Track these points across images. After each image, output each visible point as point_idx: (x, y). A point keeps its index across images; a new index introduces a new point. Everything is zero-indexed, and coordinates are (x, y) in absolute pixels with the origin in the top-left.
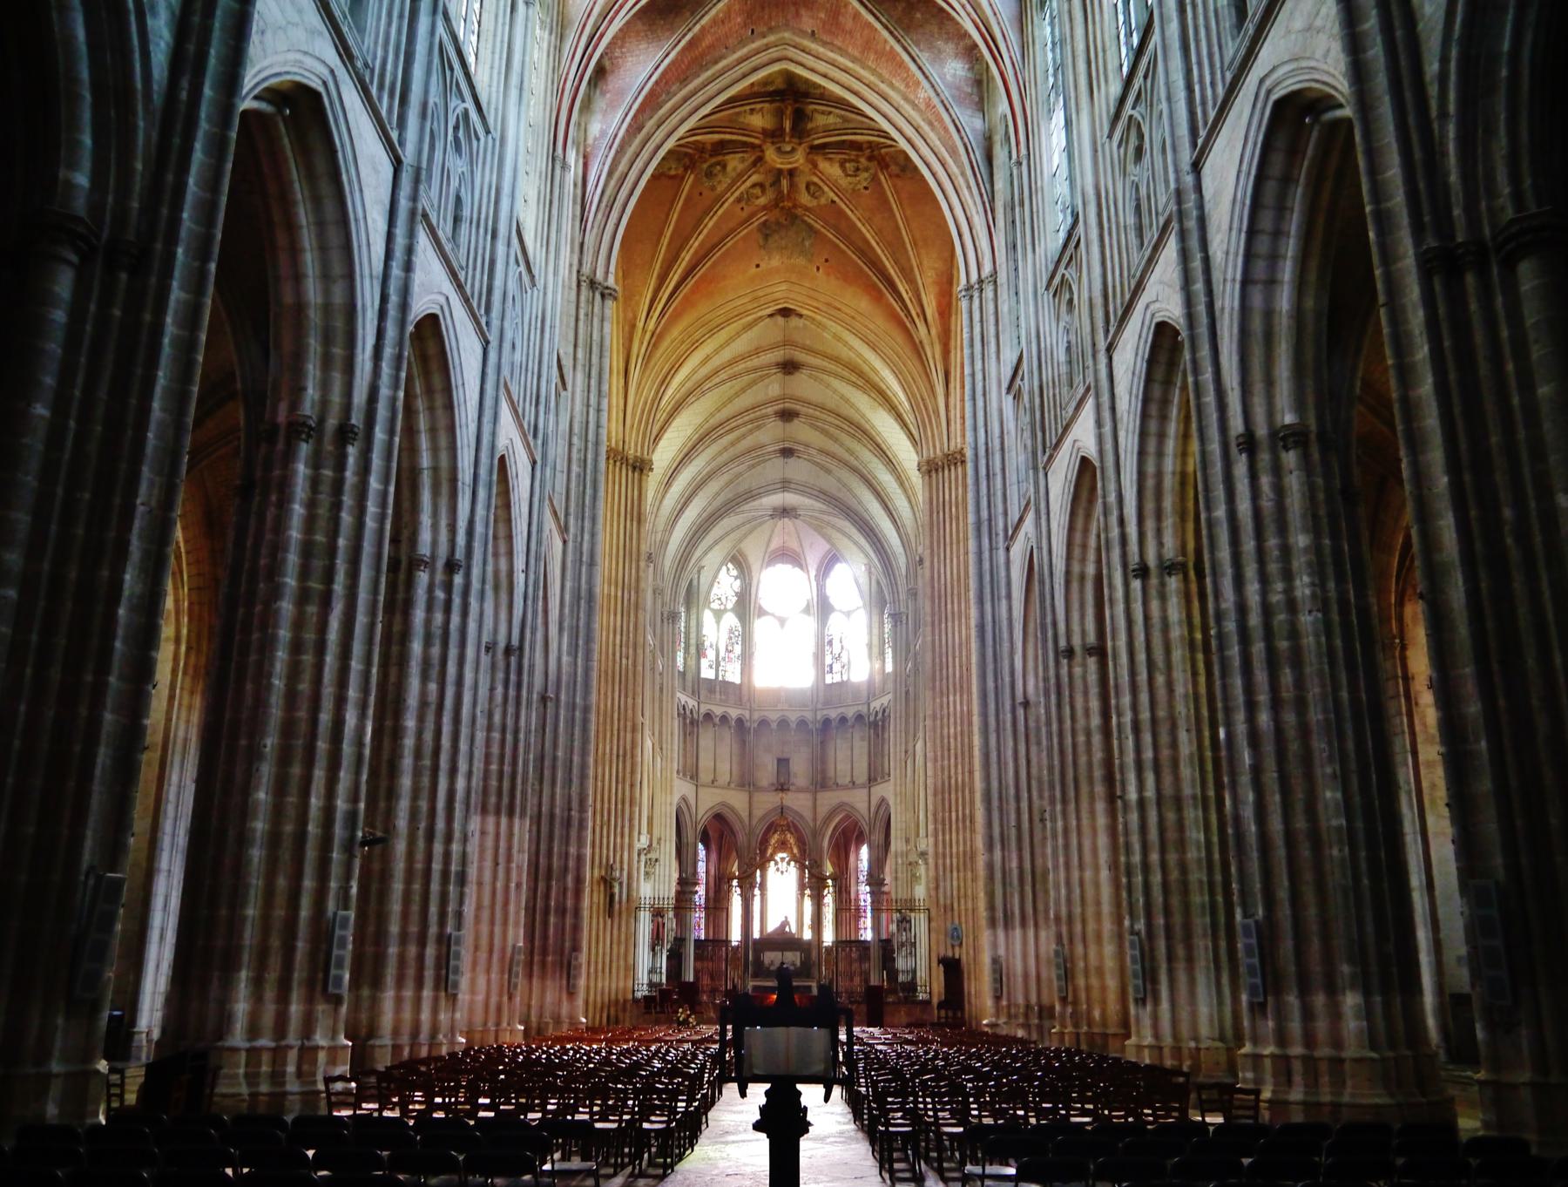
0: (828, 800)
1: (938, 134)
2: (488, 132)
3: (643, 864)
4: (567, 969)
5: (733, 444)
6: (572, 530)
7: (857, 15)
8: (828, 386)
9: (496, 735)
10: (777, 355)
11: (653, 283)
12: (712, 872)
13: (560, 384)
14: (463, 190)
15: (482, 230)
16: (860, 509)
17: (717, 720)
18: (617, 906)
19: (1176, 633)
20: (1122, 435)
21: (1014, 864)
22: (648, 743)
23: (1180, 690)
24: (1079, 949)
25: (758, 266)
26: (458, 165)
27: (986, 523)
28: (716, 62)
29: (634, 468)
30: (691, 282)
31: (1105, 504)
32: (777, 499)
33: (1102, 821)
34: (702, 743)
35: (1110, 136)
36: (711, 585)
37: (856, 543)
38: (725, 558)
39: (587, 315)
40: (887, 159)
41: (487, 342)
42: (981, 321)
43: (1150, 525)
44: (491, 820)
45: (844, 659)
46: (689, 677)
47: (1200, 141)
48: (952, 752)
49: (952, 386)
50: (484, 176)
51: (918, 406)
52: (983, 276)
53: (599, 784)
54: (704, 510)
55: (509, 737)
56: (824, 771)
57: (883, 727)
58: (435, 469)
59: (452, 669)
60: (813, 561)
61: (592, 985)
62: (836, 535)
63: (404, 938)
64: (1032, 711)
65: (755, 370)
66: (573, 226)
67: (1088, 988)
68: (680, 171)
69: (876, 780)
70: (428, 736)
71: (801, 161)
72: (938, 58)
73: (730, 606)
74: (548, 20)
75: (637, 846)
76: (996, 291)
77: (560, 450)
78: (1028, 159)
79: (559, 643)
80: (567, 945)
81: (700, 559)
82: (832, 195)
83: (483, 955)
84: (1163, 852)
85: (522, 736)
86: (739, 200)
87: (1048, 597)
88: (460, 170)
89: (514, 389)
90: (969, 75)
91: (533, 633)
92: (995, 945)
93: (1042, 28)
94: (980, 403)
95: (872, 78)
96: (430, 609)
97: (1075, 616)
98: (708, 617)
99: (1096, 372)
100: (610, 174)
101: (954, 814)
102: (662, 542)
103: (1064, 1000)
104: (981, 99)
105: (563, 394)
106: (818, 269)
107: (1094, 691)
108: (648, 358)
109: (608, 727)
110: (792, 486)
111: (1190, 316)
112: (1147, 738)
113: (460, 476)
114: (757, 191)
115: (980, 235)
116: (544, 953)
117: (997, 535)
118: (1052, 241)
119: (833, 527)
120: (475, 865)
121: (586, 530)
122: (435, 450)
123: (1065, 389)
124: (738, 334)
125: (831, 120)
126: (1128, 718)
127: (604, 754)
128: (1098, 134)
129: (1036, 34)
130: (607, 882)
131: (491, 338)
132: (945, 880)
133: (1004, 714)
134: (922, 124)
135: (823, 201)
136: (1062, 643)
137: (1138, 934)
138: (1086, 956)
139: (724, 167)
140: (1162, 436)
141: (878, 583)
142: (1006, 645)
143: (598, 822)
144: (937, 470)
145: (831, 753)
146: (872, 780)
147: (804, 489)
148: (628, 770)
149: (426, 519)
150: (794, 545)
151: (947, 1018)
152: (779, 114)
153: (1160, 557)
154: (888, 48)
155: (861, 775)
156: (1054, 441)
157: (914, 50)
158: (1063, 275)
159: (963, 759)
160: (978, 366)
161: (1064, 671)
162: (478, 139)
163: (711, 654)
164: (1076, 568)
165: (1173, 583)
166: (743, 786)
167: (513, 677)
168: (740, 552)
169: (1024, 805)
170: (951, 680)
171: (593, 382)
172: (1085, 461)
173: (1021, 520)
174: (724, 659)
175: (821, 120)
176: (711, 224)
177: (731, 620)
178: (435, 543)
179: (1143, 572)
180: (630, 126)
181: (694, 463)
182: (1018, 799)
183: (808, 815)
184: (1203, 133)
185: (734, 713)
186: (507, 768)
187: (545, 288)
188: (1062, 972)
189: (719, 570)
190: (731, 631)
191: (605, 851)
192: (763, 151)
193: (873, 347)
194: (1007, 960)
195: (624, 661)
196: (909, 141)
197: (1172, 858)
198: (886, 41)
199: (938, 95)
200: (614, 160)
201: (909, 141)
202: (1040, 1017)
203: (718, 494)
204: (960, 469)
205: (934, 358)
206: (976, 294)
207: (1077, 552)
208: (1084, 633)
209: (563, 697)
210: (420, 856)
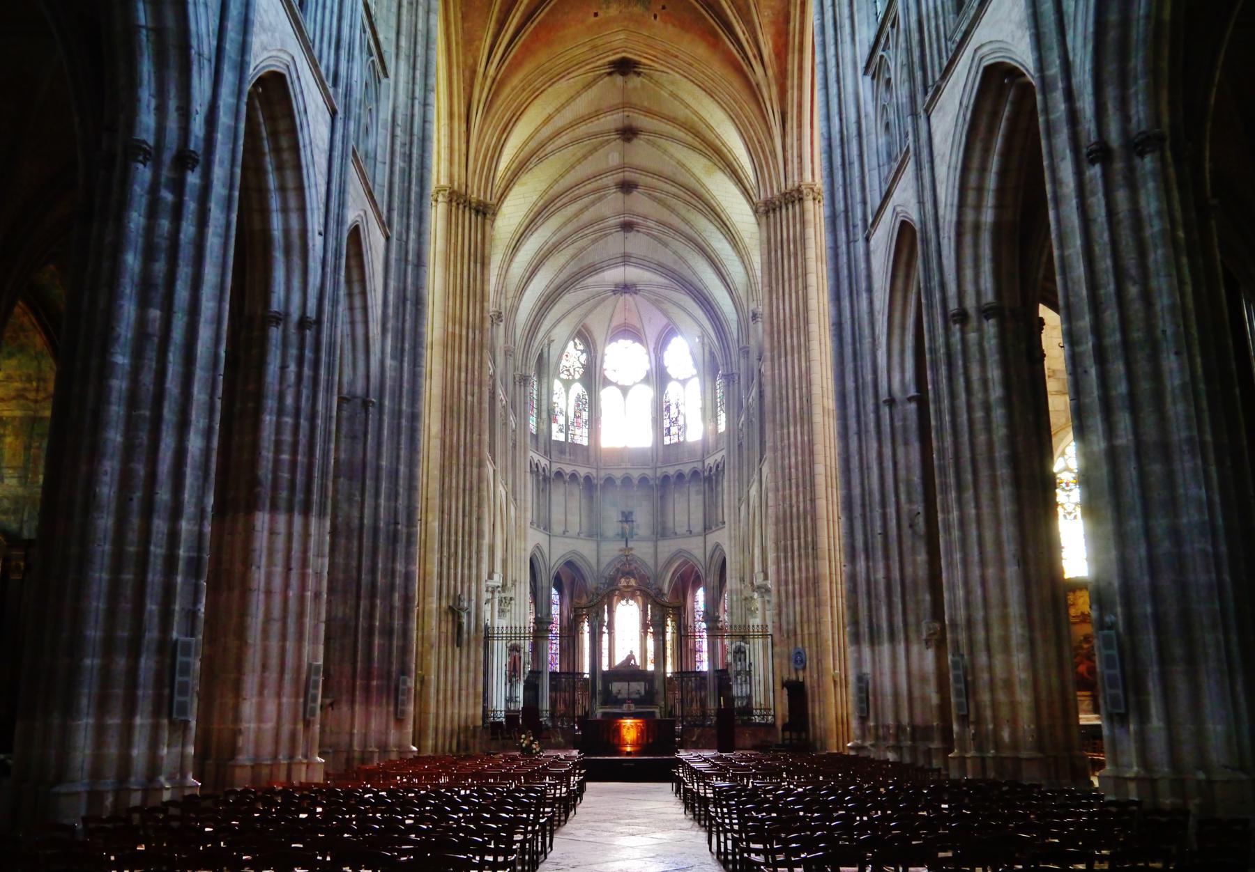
3: (496, 601)
5: (576, 215)
6: (396, 226)
8: (665, 152)
9: (288, 420)
10: (619, 176)
11: (492, 26)
12: (565, 614)
13: (379, 67)
16: (695, 281)
17: (567, 478)
18: (465, 636)
21: (880, 575)
22: (501, 489)
25: (596, 15)
27: (842, 215)
29: (477, 212)
30: (531, 27)
32: (615, 274)
34: (553, 497)
36: (560, 357)
37: (690, 315)
38: (572, 332)
44: (282, 519)
45: (681, 422)
46: (542, 440)
48: (794, 481)
49: (788, 126)
51: (755, 148)
53: (446, 517)
54: (552, 282)
56: (663, 523)
57: (717, 482)
58: (158, 31)
59: (182, 293)
60: (651, 333)
62: (674, 311)
63: (109, 646)
64: (899, 409)
65: (595, 135)
70: (147, 378)
73: (577, 376)
77: (381, 140)
80: (394, 668)
81: (549, 331)
83: (273, 676)
87: (934, 255)
89: (309, 27)
91: (335, 303)
92: (859, 662)
94: (833, 90)
96: (152, 213)
97: (969, 274)
98: (557, 385)
101: (796, 542)
102: (512, 307)
105: (384, 81)
106: (655, 17)
108: (489, 105)
109: (454, 462)
110: (633, 260)
112: (1118, 368)
113: (194, 43)
117: (855, 226)
119: (670, 301)
120: (263, 570)
121: (412, 227)
127: (450, 487)
130: (454, 612)
132: (787, 606)
133: (866, 415)
136: (953, 305)
137: (1112, 626)
141: (711, 353)
142: (867, 342)
143: (445, 554)
145: (670, 506)
146: (707, 528)
147: (644, 263)
148: (475, 504)
149: (146, 96)
150: (634, 321)
153: (1125, 132)
155: (698, 526)
156: (945, 63)
159: (805, 488)
160: (831, 51)
161: (956, 337)
163: (561, 420)
164: (970, 217)
165: (1148, 163)
166: (590, 535)
167: (308, 354)
168: (584, 326)
169: (891, 511)
170: (791, 412)
174: (573, 424)
177: (578, 389)
178: (161, 130)
182: (884, 504)
183: (650, 562)
185: (582, 472)
190: (578, 398)
191: (452, 582)
195: (469, 398)
197: (1160, 524)
203: (564, 267)
204: (797, 207)
205: (771, 99)
207: (971, 197)
209: (387, 403)
210: (133, 536)
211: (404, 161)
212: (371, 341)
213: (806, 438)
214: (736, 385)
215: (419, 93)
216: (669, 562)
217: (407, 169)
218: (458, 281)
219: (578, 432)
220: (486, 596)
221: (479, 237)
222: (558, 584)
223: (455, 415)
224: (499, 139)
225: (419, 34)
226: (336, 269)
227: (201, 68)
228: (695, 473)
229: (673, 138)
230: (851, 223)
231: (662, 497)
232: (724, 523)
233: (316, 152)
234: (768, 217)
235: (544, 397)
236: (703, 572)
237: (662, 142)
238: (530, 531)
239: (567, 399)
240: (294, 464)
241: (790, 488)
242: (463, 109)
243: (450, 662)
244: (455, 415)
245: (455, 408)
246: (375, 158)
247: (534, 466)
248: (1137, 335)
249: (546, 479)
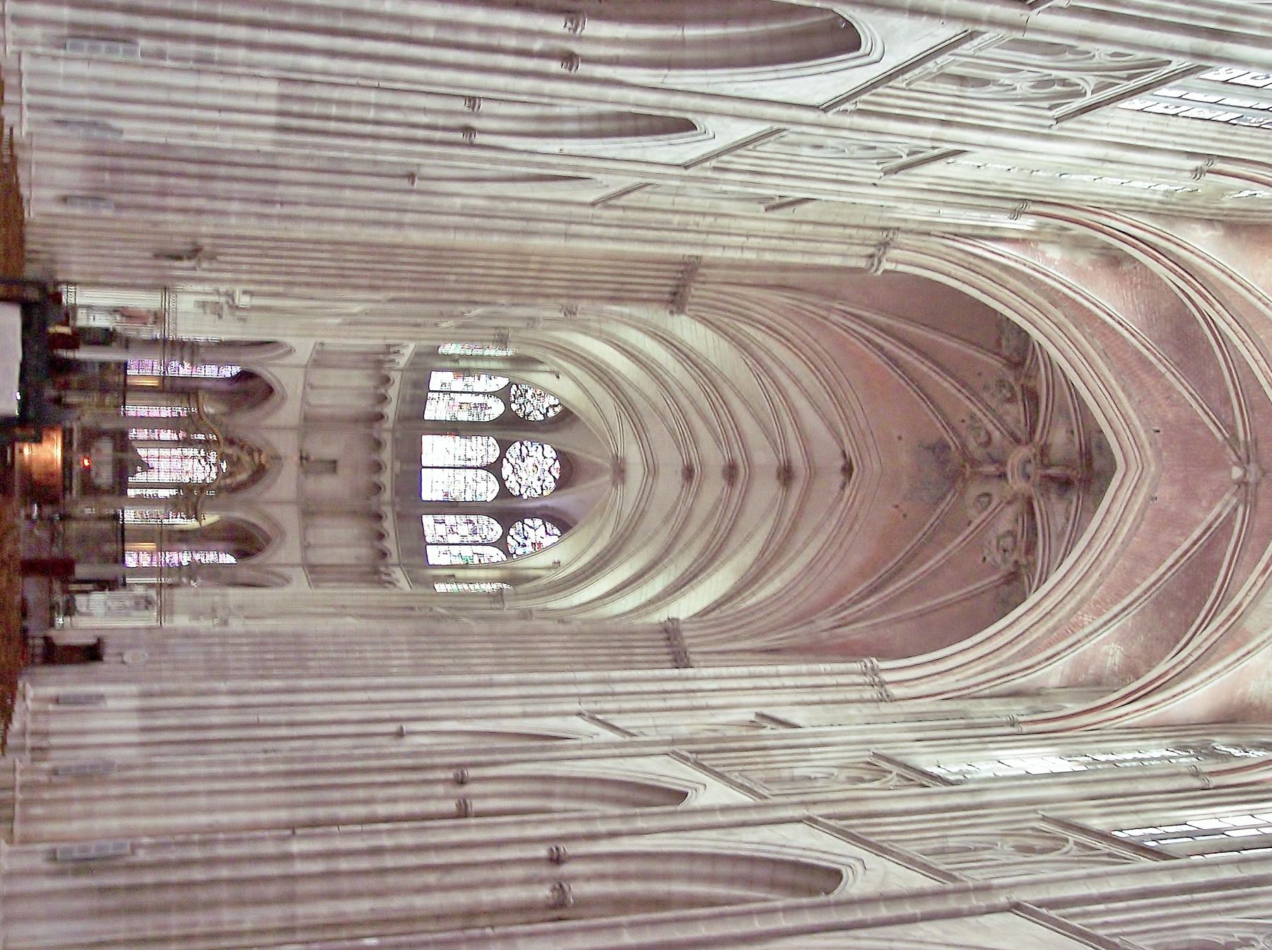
0: (288, 518)
1: (1044, 636)
2: (1058, 120)
3: (215, 298)
4: (95, 197)
5: (700, 412)
7: (1175, 547)
8: (764, 518)
9: (371, 114)
11: (882, 320)
13: (773, 203)
14: (996, 88)
15: (950, 109)
16: (623, 556)
18: (167, 263)
19: (486, 897)
20: (713, 834)
21: (215, 719)
22: (356, 308)
23: (420, 901)
24: (115, 790)
25: (900, 438)
26: (1023, 85)
28: (1123, 389)
29: (674, 294)
31: (635, 816)
33: (265, 816)
35: (1044, 819)
38: (567, 402)
39: (850, 237)
40: (1015, 583)
41: (825, 110)
42: (838, 685)
43: (610, 867)
47: (1044, 911)
50: (1009, 114)
52: (887, 687)
54: (624, 378)
55: (369, 129)
58: (683, 43)
60: (566, 501)
61: (75, 233)
66: (948, 224)
67: (70, 800)
68: (1006, 352)
69: (311, 572)
71: (1015, 488)
72: (1125, 637)
73: (514, 407)
74: (1174, 200)
75: (238, 289)
76: (872, 701)
77: (697, 201)
78: (1015, 733)
79: (474, 196)
80: (123, 198)
82: (977, 521)
84: (231, 882)
85: (369, 144)
86: (973, 417)
88: (1018, 85)
89: (770, 147)
90: (1107, 672)
91: (490, 161)
93: (1160, 746)
95: (1105, 564)
99: (785, 805)
100: (1005, 268)
102: (588, 327)
103: (55, 772)
104: (1081, 685)
105: (762, 207)
106: (897, 506)
107: (417, 808)
109: (376, 258)
110: (650, 480)
111: (851, 903)
112: (364, 864)
113: (674, 72)
114: (983, 438)
115: (933, 684)
116: (115, 170)
118: (927, 761)
122: (704, 43)
123: (762, 775)
124: (823, 417)
125: (1060, 520)
126: (387, 842)
128: (1047, 806)
129: (1153, 742)
130: (195, 252)
131: (830, 114)
134: (1056, 619)
135: (972, 512)
136: (472, 773)
137: (133, 853)
138: (105, 798)
139: (1010, 400)
140: (711, 879)
143: (266, 244)
144: (669, 639)
147: (646, 495)
151: (34, 647)
152: (1067, 464)
153: (573, 878)
154: (1138, 581)
155: (316, 557)
156: (705, 763)
157: (1134, 611)
158: (891, 772)
161: (441, 775)
162: (1050, 108)
163: (458, 385)
164: (558, 788)
167: (438, 135)
169: (284, 732)
171: (774, 242)
172: (684, 795)
173: (613, 728)
175: (1059, 507)
176: (946, 384)
179: (556, 860)
180: (1058, 292)
181: (679, 367)
182: (292, 724)
184: (1053, 913)
185: (390, 410)
186: (332, 125)
187: (883, 186)
188: (88, 770)
189: (556, 396)
191: (232, 251)
192: (1027, 443)
193: (810, 567)
194: (102, 711)
195: (452, 278)
196: (1037, 604)
198: (1145, 579)
199: (1087, 636)
200: (1023, 273)
201: (1037, 604)
202: (33, 749)
206: (867, 679)
207: (578, 789)
208: (484, 796)
209: (414, 199)
211: (679, 224)
212: (478, 184)
213: (395, 670)
214: (489, 606)
215: (753, 242)
216: (267, 518)
217: (671, 227)
218: (591, 270)
219: (442, 404)
220: (223, 288)
221: (645, 296)
222: (245, 376)
223: (432, 261)
224: (759, 322)
225: (818, 245)
226: (526, 164)
227: (654, 76)
228: (384, 554)
229: (776, 528)
230: (600, 698)
231: (353, 514)
232: (317, 587)
233: (640, 151)
234: (661, 632)
235: (486, 365)
236: (254, 561)
237: (774, 514)
238: (311, 343)
239: (484, 393)
240: (328, 118)
241: (336, 651)
242: (791, 282)
243: (136, 245)
244: (432, 261)
245: (441, 261)
246: (677, 195)
247: (396, 349)
248: (391, 880)
249: (379, 364)
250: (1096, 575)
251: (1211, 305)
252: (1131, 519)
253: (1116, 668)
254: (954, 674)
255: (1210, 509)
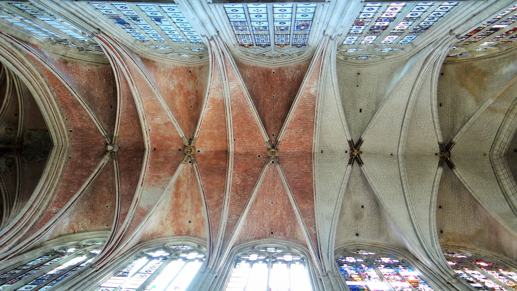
1: (39, 219)
28: (62, 114)
95: (55, 185)
134: (41, 211)
196: (31, 206)
201: (31, 206)
250: (53, 190)
251: (133, 86)
252: (62, 166)
253: (66, 227)
254: (6, 245)
255: (99, 162)
